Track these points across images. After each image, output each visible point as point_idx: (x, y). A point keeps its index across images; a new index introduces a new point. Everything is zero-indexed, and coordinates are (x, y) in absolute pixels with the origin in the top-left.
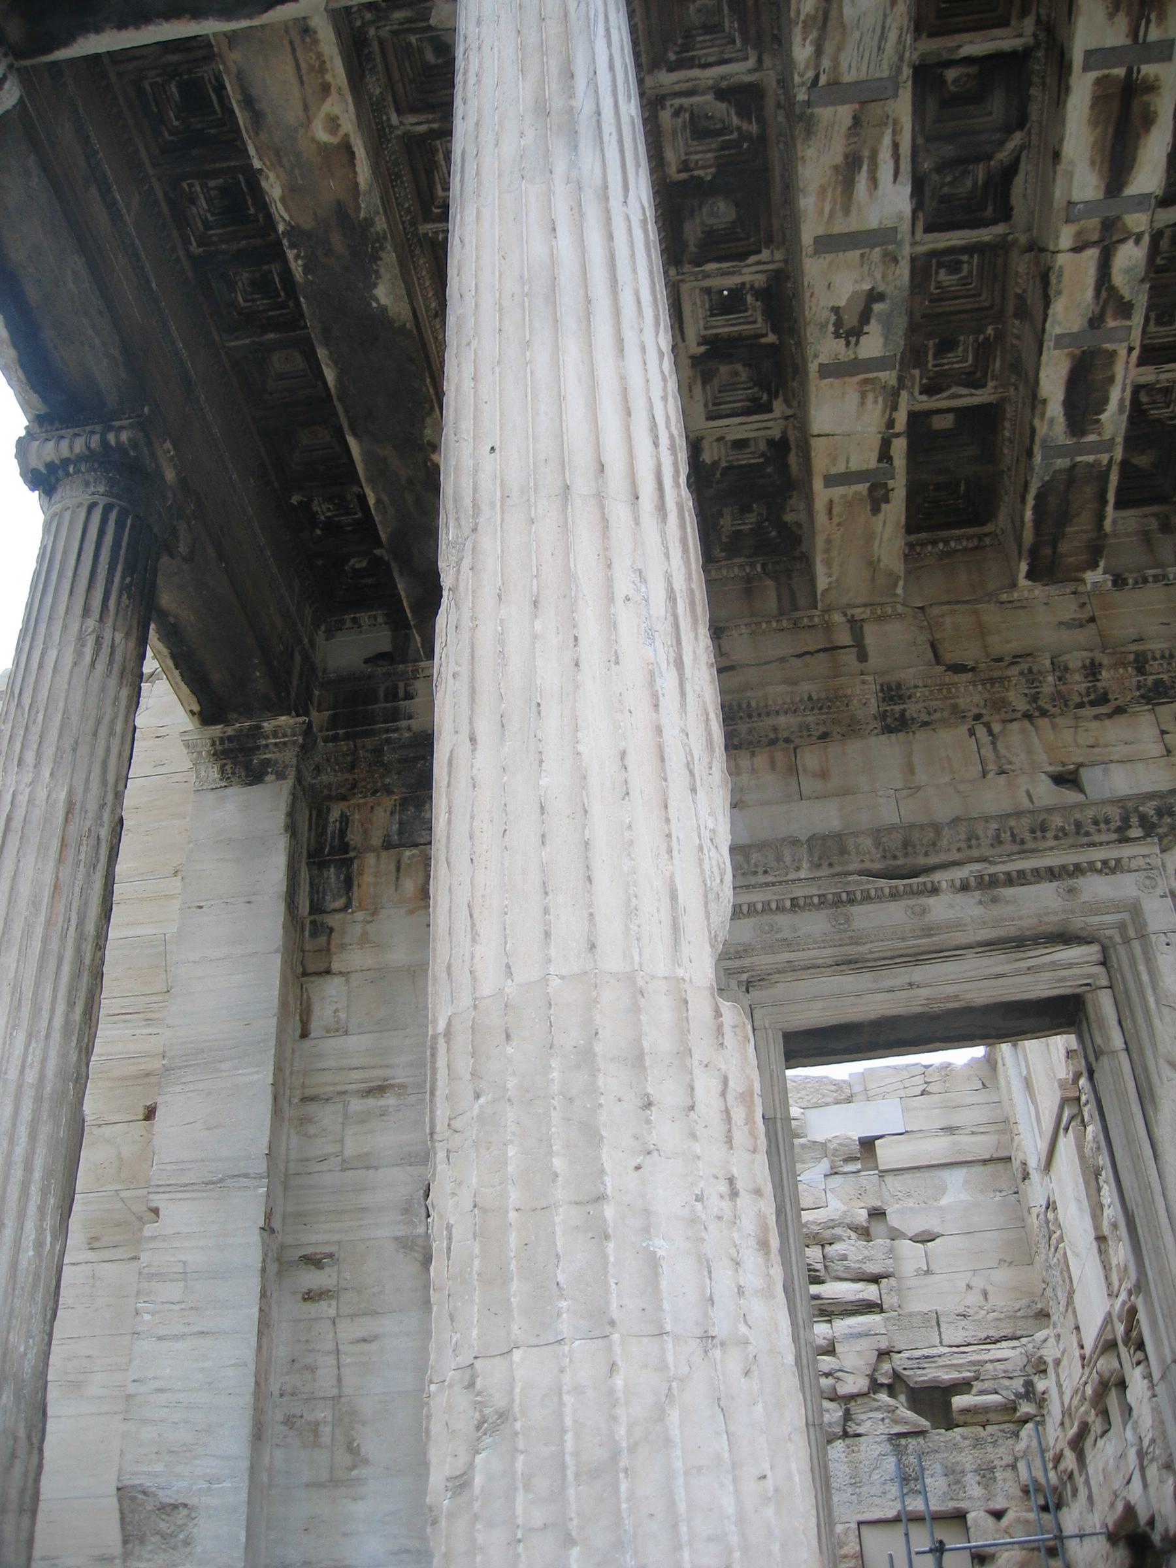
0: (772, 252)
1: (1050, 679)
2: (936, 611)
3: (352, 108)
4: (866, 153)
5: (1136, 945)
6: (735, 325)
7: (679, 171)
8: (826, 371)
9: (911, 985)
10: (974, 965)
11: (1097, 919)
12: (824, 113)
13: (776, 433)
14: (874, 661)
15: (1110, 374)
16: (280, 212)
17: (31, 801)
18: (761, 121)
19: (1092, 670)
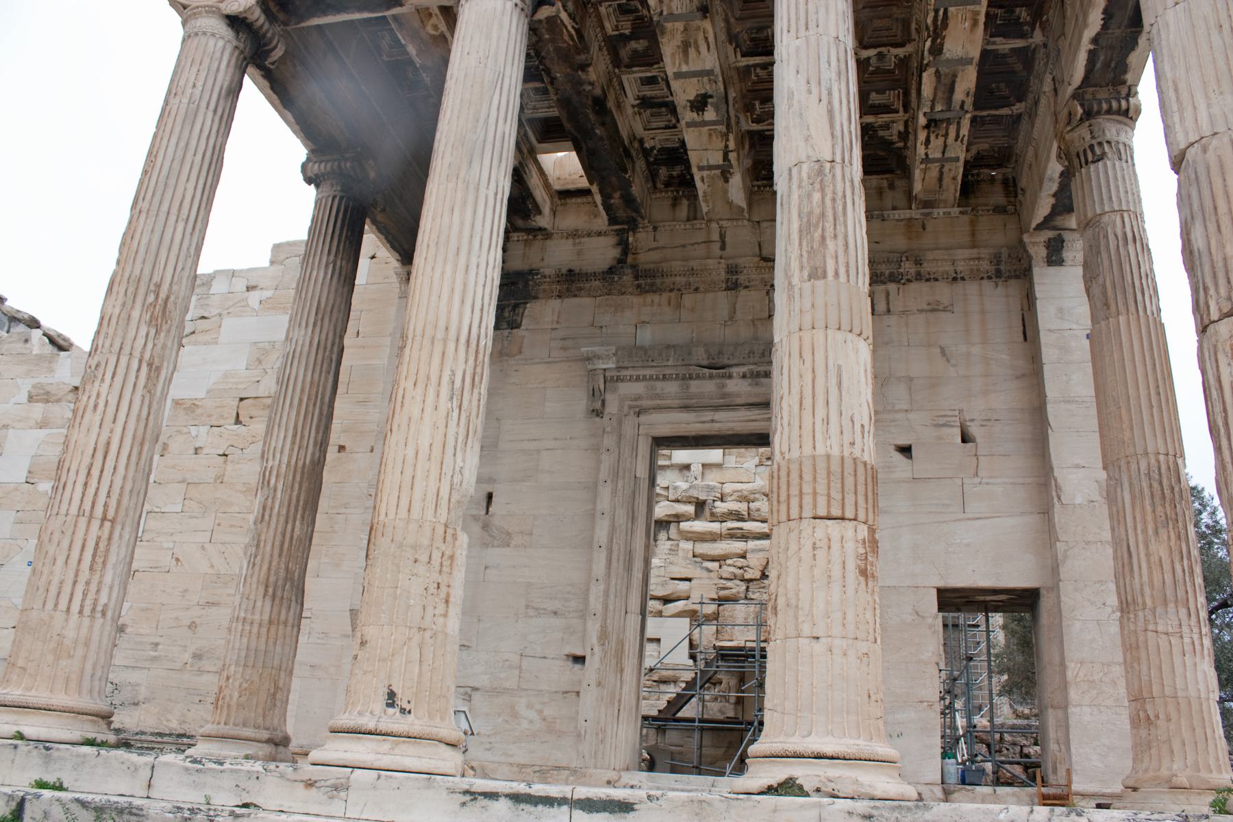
8: (689, 125)
9: (712, 421)
10: (743, 414)
12: (669, 25)
14: (729, 250)
16: (417, 60)
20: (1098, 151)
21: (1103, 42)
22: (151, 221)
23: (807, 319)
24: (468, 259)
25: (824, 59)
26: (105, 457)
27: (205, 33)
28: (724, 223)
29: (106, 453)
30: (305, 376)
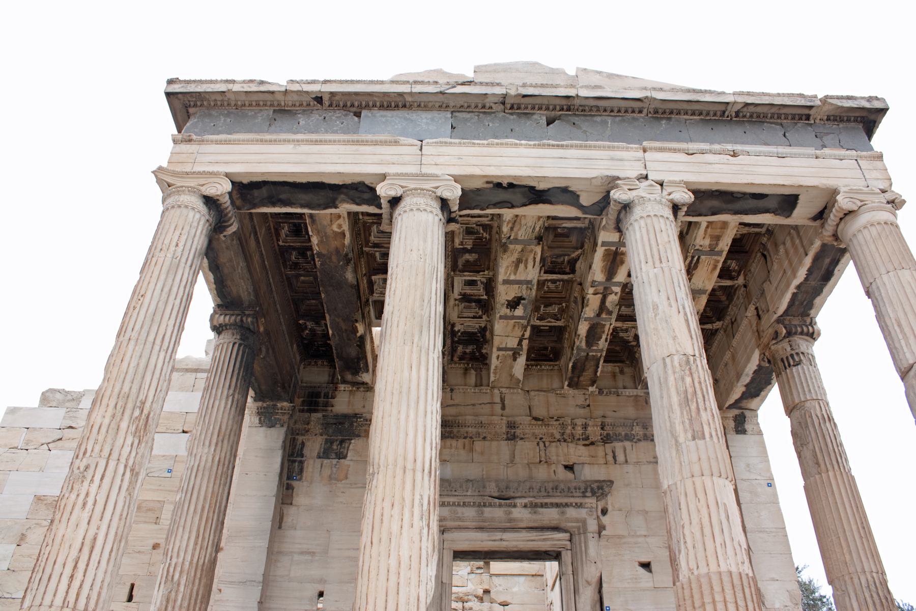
1: (570, 427)
2: (532, 393)
5: (582, 536)
8: (501, 317)
10: (524, 535)
11: (570, 524)
12: (511, 247)
13: (483, 325)
14: (507, 411)
16: (316, 248)
17: (206, 461)
19: (585, 427)
20: (797, 359)
21: (803, 289)
22: (139, 349)
23: (696, 469)
24: (426, 408)
25: (676, 284)
26: (91, 552)
27: (186, 207)
28: (504, 390)
29: (92, 548)
30: (207, 487)
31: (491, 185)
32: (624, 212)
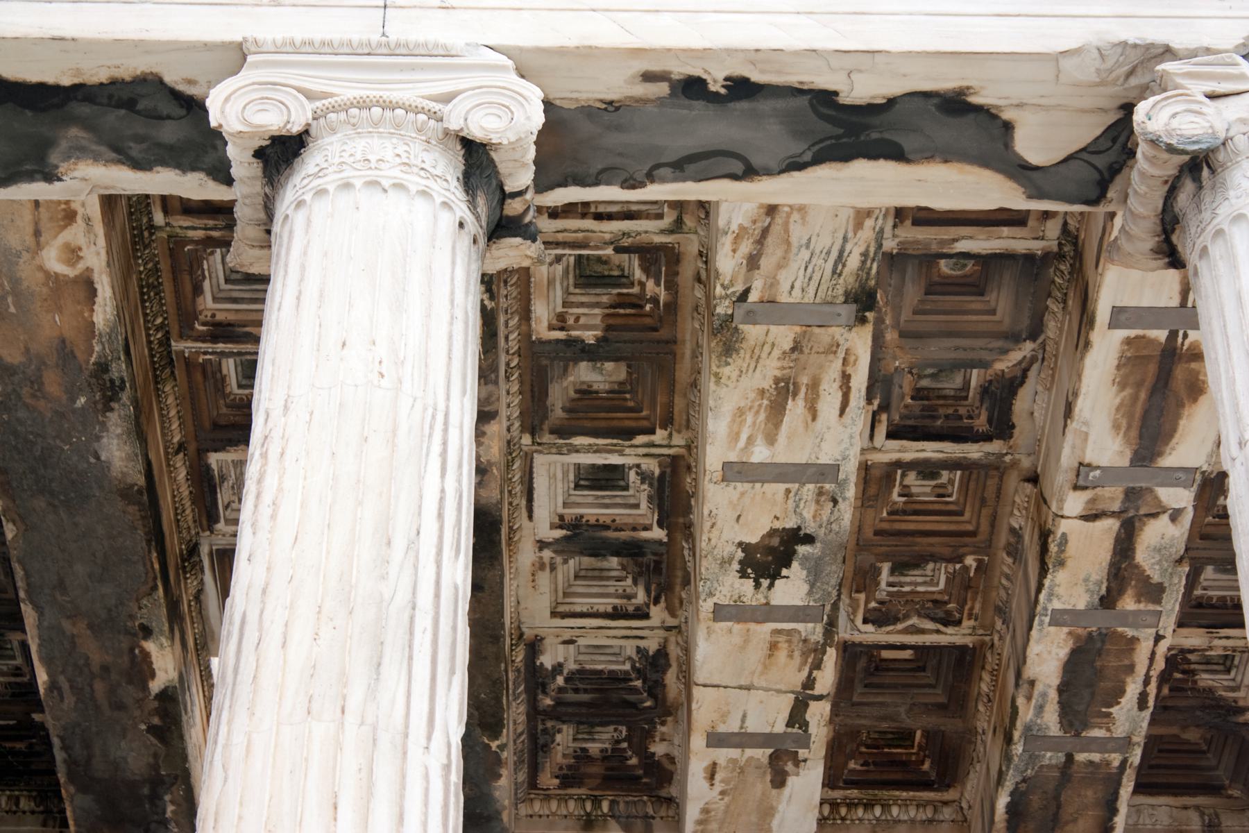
0: (670, 435)
3: (102, 241)
4: (804, 380)
6: (607, 506)
7: (551, 328)
12: (753, 332)
13: (652, 646)
15: (1127, 662)
18: (671, 286)
31: (663, 89)
32: (1188, 186)
